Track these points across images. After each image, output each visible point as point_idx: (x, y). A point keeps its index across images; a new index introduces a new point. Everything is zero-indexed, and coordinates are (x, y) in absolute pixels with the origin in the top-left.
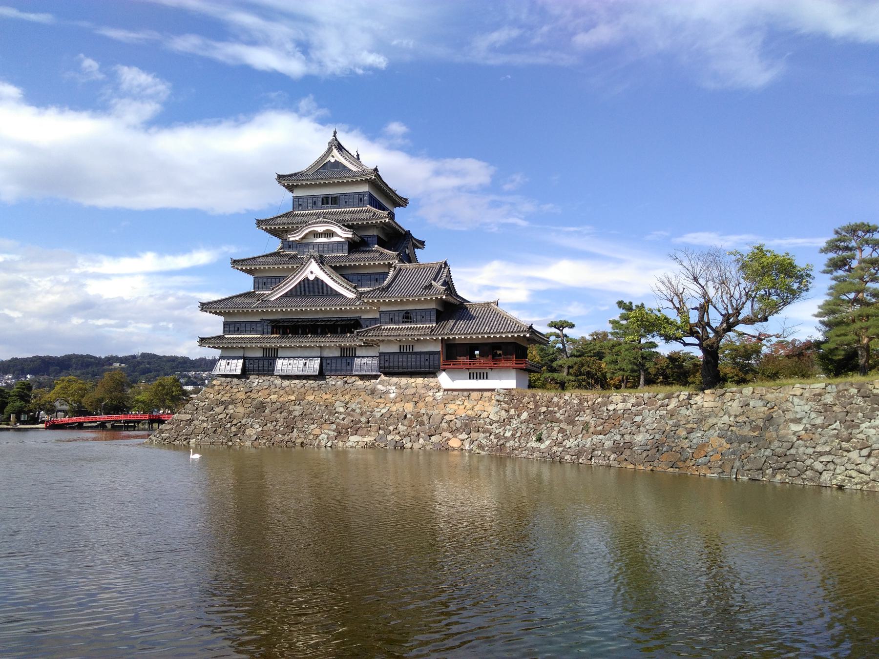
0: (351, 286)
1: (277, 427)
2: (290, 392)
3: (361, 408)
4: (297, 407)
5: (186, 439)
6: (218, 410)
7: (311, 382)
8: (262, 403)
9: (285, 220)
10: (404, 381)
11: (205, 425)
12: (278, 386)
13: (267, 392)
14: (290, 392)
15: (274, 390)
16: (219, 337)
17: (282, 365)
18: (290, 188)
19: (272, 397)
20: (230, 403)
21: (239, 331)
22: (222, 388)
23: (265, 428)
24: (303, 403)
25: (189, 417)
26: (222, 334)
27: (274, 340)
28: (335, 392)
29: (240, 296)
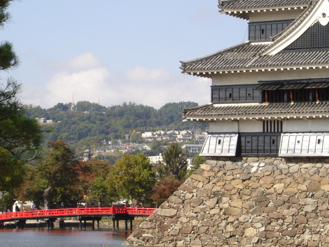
1: (285, 227)
2: (300, 180)
4: (309, 200)
5: (172, 241)
11: (194, 222)
12: (285, 172)
13: (270, 179)
14: (300, 180)
15: (279, 177)
16: (206, 107)
17: (289, 144)
19: (277, 186)
20: (223, 195)
21: (231, 98)
23: (269, 228)
24: (317, 194)
25: (173, 212)
26: (210, 103)
27: (275, 113)
29: (231, 50)
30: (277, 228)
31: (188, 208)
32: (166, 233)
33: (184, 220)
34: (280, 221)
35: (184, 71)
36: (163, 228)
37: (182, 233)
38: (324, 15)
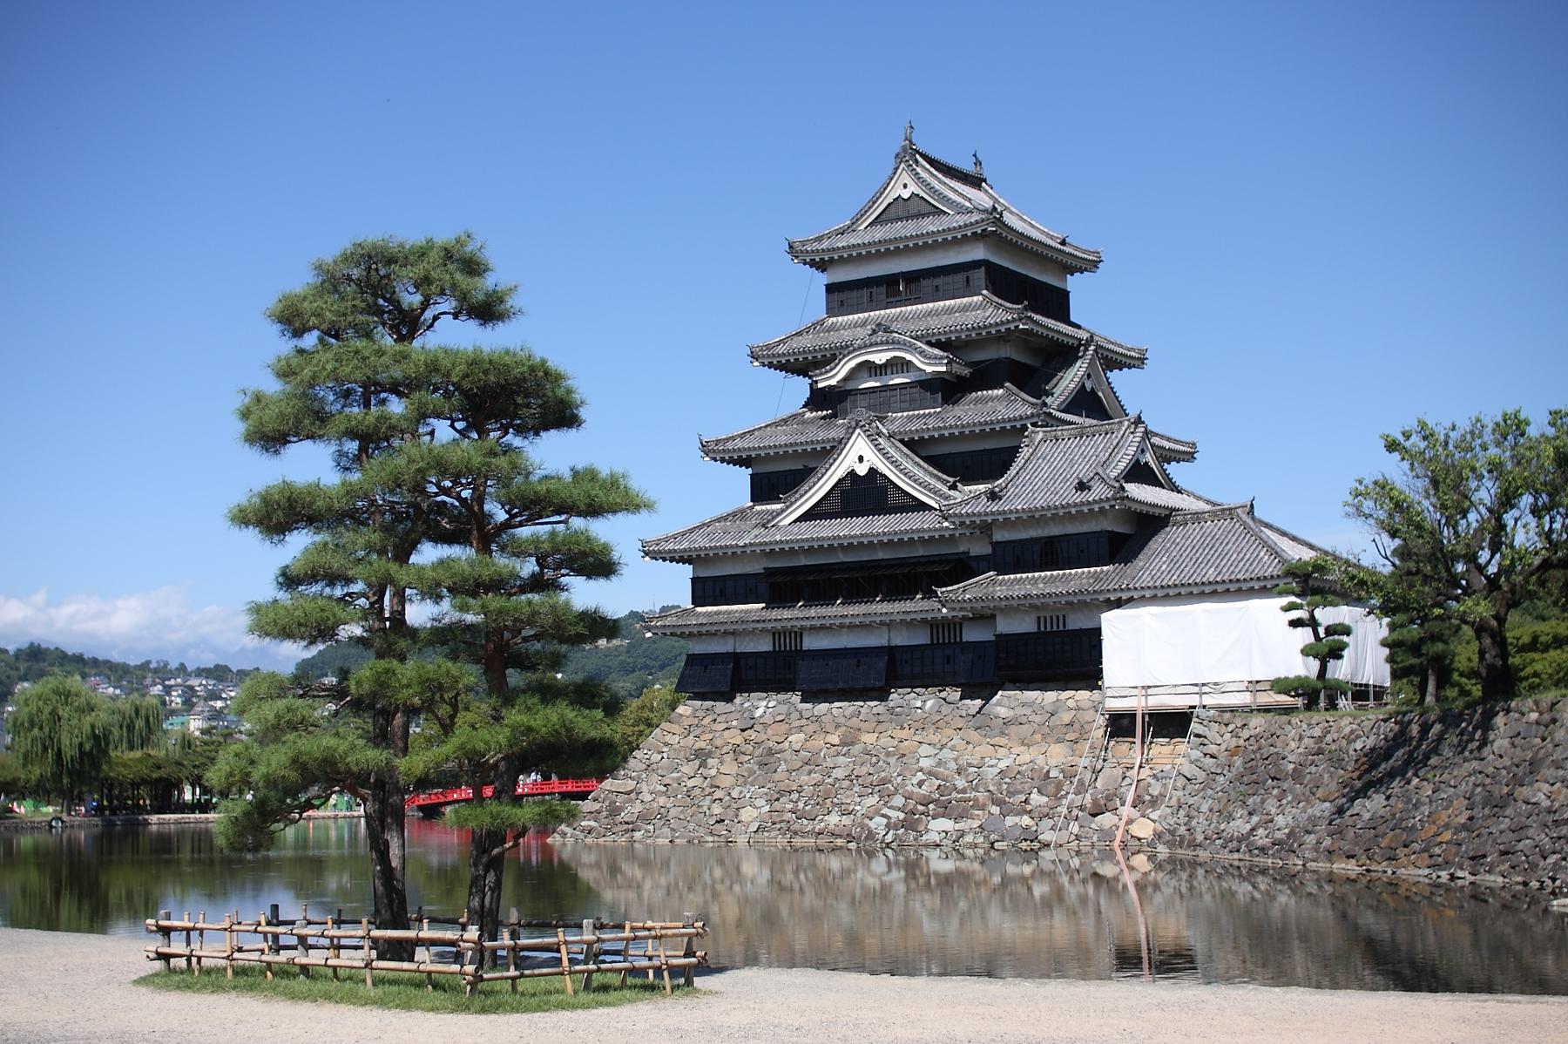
0: (944, 482)
1: (801, 805)
3: (956, 760)
5: (626, 831)
6: (687, 769)
7: (872, 704)
8: (770, 752)
9: (807, 342)
10: (1051, 696)
11: (662, 800)
12: (806, 714)
13: (783, 727)
15: (797, 723)
18: (821, 266)
20: (710, 755)
22: (696, 721)
24: (856, 749)
25: (631, 784)
28: (919, 725)
29: (718, 520)
30: (790, 806)
31: (655, 778)
32: (619, 819)
33: (648, 798)
34: (795, 796)
35: (647, 554)
36: (614, 811)
37: (644, 817)
38: (861, 459)
